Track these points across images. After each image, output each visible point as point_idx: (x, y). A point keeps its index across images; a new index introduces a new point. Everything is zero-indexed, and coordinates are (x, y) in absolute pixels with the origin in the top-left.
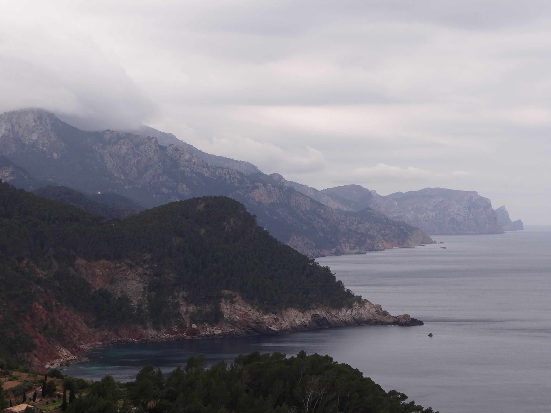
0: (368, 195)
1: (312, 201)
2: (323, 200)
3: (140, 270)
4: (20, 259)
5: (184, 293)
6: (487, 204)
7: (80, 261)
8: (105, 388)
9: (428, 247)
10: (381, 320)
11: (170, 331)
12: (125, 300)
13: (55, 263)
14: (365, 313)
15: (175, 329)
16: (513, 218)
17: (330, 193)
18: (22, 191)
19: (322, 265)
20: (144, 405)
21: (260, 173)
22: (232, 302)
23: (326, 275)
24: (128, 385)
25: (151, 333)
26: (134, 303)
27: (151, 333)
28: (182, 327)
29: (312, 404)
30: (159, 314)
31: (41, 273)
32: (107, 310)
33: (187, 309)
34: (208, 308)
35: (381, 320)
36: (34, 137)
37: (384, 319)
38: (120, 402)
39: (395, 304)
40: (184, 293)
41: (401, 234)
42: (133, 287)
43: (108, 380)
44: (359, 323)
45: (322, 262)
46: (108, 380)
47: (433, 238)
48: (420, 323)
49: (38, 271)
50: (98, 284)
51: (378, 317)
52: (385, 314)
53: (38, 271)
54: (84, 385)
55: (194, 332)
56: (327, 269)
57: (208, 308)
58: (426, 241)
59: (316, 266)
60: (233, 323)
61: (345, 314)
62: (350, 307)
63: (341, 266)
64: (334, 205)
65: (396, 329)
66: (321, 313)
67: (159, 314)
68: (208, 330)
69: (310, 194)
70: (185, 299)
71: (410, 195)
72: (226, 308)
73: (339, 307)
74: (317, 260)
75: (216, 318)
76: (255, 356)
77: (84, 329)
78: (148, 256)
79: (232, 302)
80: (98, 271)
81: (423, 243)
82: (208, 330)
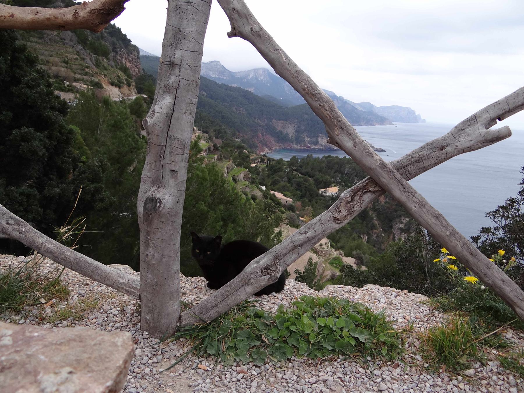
0: (372, 106)
1: (353, 107)
2: (357, 107)
3: (293, 125)
4: (255, 118)
5: (307, 134)
6: (414, 113)
7: (274, 120)
8: (280, 161)
9: (391, 126)
11: (301, 146)
12: (287, 134)
13: (266, 121)
15: (303, 145)
16: (423, 118)
17: (359, 104)
18: (257, 96)
20: (292, 168)
21: (336, 96)
22: (322, 138)
24: (287, 161)
25: (295, 146)
26: (290, 136)
27: (295, 146)
28: (305, 145)
29: (347, 173)
30: (298, 140)
31: (261, 123)
32: (281, 138)
33: (307, 139)
34: (314, 139)
36: (262, 78)
38: (285, 167)
40: (307, 134)
41: (382, 120)
42: (290, 131)
43: (281, 159)
46: (281, 159)
47: (393, 123)
48: (385, 151)
49: (260, 122)
50: (279, 129)
53: (260, 122)
54: (273, 160)
55: (309, 147)
57: (314, 139)
58: (390, 123)
60: (322, 145)
64: (360, 108)
67: (298, 140)
68: (313, 147)
69: (352, 104)
70: (307, 136)
71: (387, 107)
72: (320, 140)
75: (316, 143)
76: (329, 156)
77: (274, 142)
78: (296, 121)
79: (322, 138)
80: (280, 125)
81: (389, 124)
82: (313, 147)
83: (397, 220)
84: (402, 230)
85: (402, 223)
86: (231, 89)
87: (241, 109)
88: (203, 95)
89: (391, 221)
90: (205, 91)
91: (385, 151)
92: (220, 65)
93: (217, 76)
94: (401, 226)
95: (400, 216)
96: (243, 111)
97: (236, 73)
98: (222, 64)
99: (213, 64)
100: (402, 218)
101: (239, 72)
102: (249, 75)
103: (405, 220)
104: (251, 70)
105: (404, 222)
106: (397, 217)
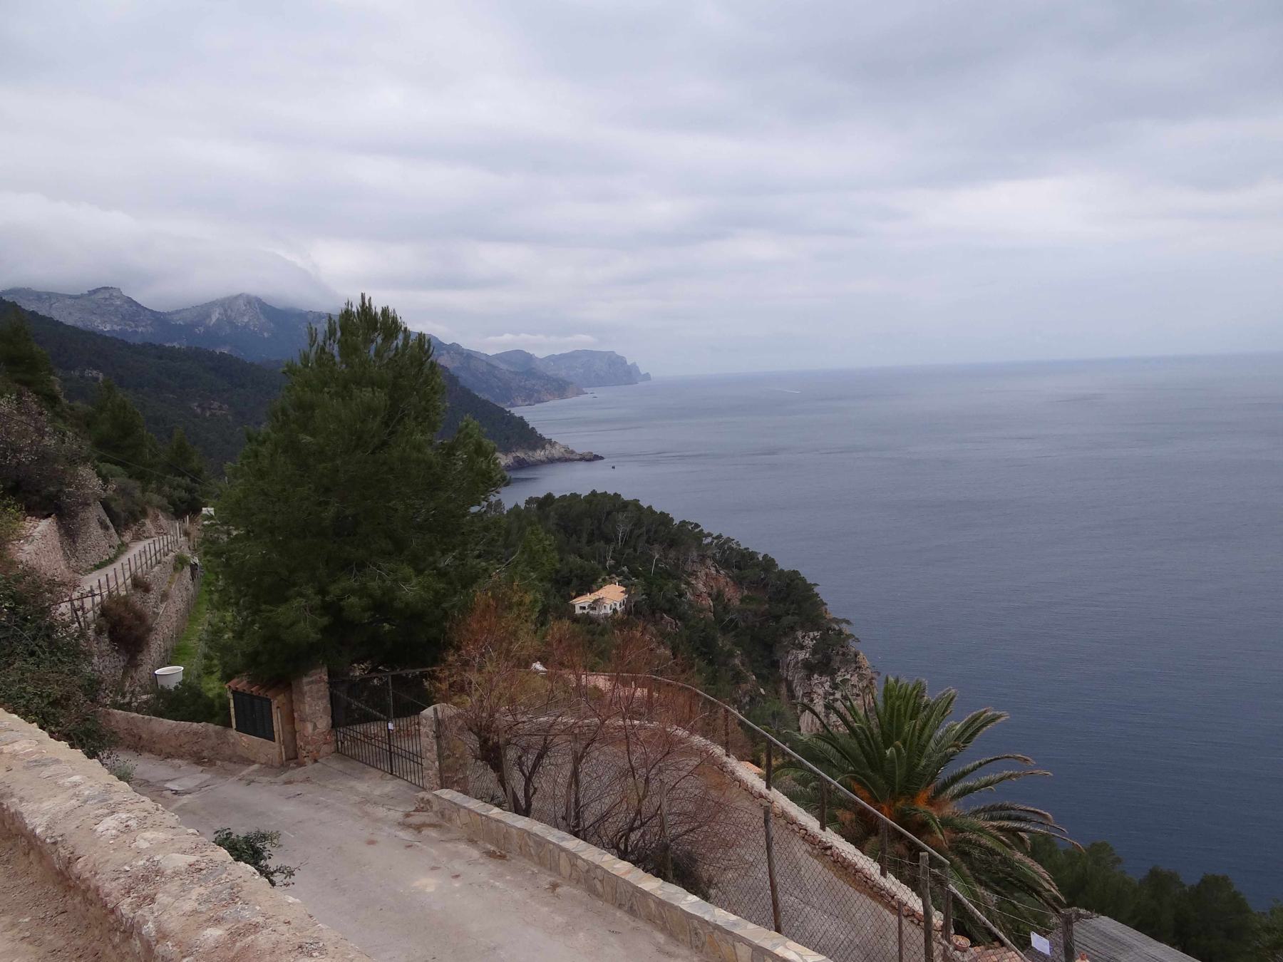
10: (568, 458)
14: (557, 452)
19: (517, 415)
23: (521, 423)
35: (568, 458)
36: (246, 319)
37: (572, 456)
39: (580, 444)
44: (552, 461)
45: (517, 412)
48: (602, 458)
51: (567, 456)
52: (572, 452)
56: (521, 418)
59: (512, 416)
61: (540, 454)
62: (543, 448)
63: (531, 414)
65: (583, 465)
66: (521, 454)
73: (534, 449)
74: (513, 410)
83: (785, 641)
84: (809, 668)
85: (802, 647)
86: (173, 354)
87: (216, 404)
88: (96, 379)
89: (769, 647)
90: (97, 368)
91: (602, 458)
92: (121, 297)
93: (117, 328)
94: (802, 655)
95: (792, 629)
96: (220, 408)
97: (169, 314)
98: (125, 293)
99: (100, 296)
100: (800, 634)
101: (178, 312)
102: (209, 316)
103: (810, 639)
104: (213, 304)
105: (808, 642)
106: (785, 634)
